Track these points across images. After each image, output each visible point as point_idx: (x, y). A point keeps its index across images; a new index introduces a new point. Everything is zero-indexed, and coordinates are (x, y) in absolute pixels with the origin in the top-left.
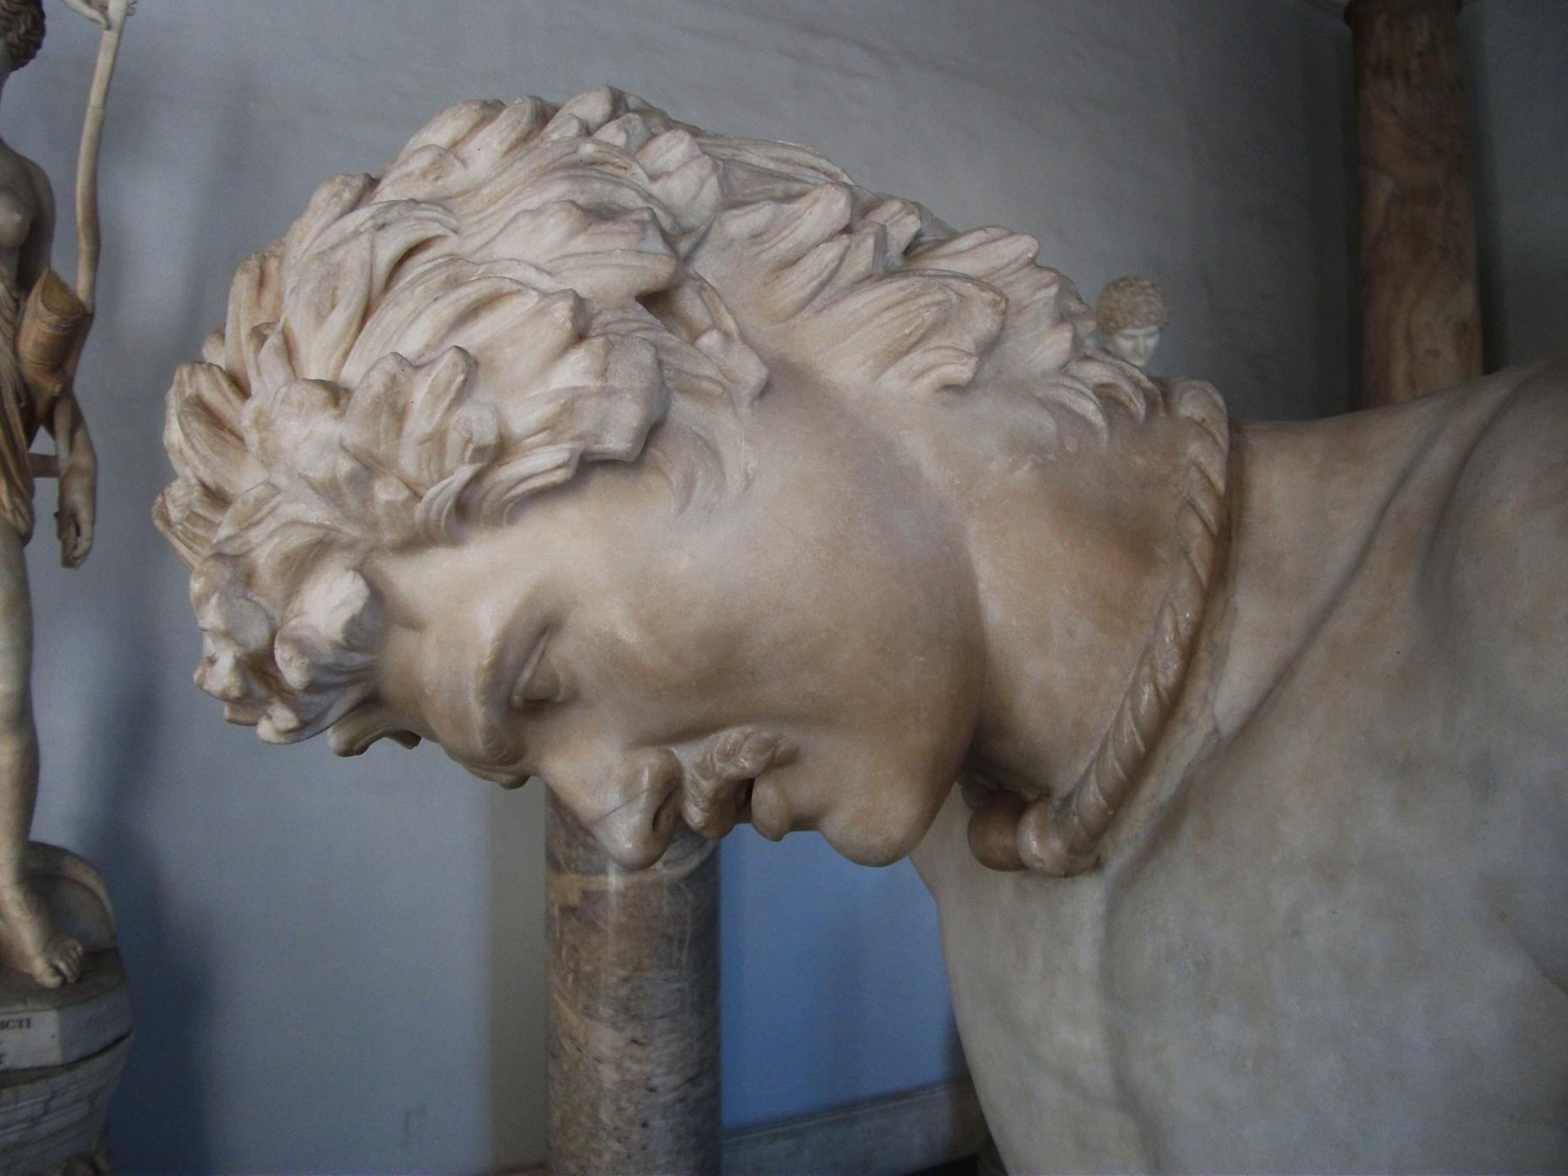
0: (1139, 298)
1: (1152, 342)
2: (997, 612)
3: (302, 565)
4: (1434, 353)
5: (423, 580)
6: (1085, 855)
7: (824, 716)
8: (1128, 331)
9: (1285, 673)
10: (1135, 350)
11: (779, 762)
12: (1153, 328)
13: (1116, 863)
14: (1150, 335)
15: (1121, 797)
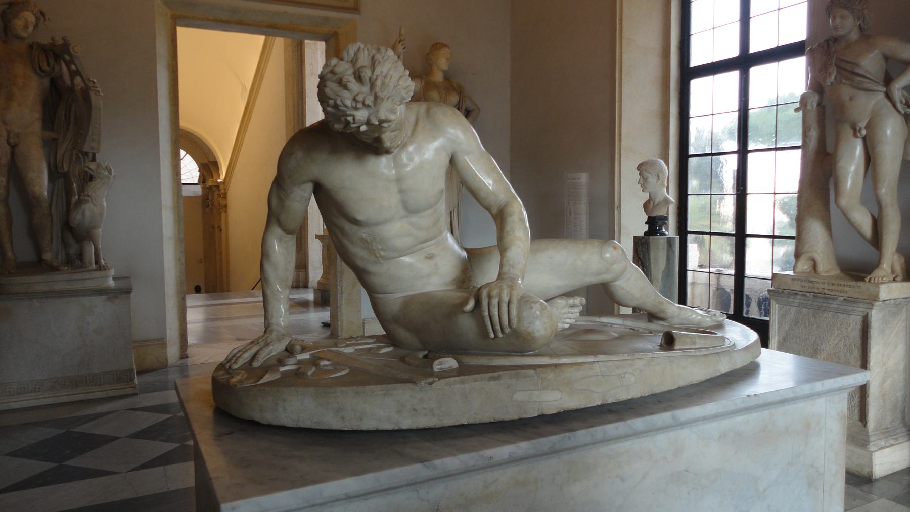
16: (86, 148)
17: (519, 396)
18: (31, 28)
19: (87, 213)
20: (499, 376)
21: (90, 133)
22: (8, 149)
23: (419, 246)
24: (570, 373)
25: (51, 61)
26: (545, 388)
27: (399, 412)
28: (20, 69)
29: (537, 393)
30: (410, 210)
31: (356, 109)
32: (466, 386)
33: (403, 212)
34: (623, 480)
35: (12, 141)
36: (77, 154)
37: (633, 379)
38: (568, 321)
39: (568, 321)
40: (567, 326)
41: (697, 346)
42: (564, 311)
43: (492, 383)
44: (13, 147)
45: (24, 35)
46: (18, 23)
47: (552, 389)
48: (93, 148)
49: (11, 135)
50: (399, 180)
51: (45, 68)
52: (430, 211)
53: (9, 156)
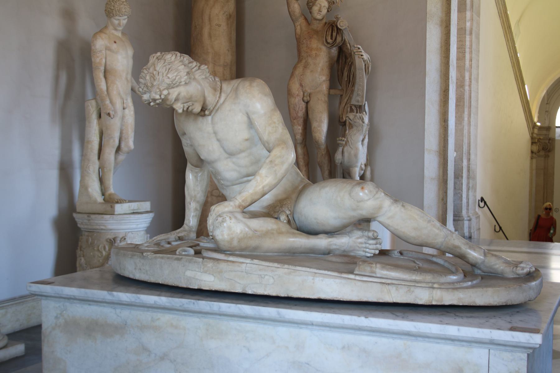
0: (122, 6)
1: (125, 22)
2: (206, 94)
3: (164, 90)
4: (219, 26)
5: (171, 91)
6: (210, 115)
7: (196, 101)
8: (117, 18)
9: (226, 99)
10: (119, 25)
11: (193, 105)
12: (126, 17)
13: (212, 114)
14: (124, 19)
15: (214, 109)
16: (353, 102)
17: (189, 273)
18: (324, 11)
19: (346, 154)
20: (181, 258)
21: (356, 89)
22: (303, 105)
23: (246, 179)
24: (223, 266)
25: (334, 34)
26: (205, 272)
27: (135, 269)
28: (315, 43)
29: (199, 274)
30: (231, 154)
31: (145, 93)
32: (163, 261)
33: (226, 155)
34: (249, 350)
35: (305, 99)
36: (351, 107)
37: (271, 281)
38: (367, 250)
39: (367, 250)
40: (369, 255)
41: (378, 275)
42: (360, 240)
43: (176, 262)
44: (307, 103)
45: (319, 17)
46: (315, 9)
47: (209, 274)
48: (358, 101)
49: (305, 94)
50: (215, 133)
51: (330, 40)
52: (243, 154)
53: (304, 110)
